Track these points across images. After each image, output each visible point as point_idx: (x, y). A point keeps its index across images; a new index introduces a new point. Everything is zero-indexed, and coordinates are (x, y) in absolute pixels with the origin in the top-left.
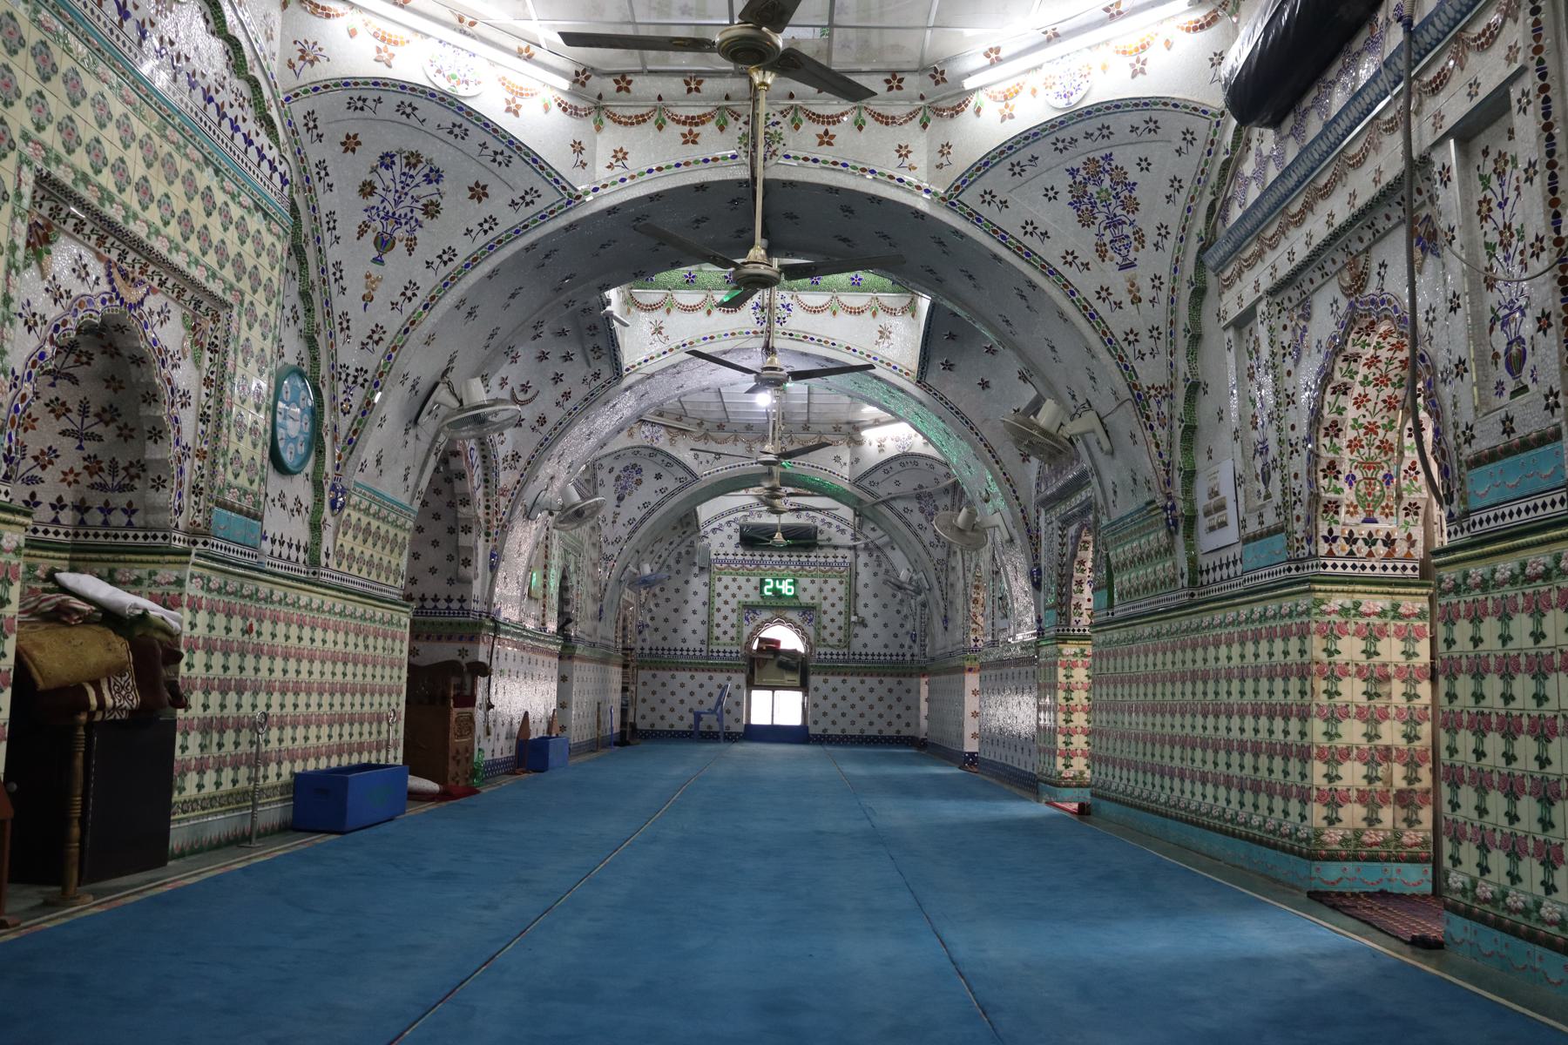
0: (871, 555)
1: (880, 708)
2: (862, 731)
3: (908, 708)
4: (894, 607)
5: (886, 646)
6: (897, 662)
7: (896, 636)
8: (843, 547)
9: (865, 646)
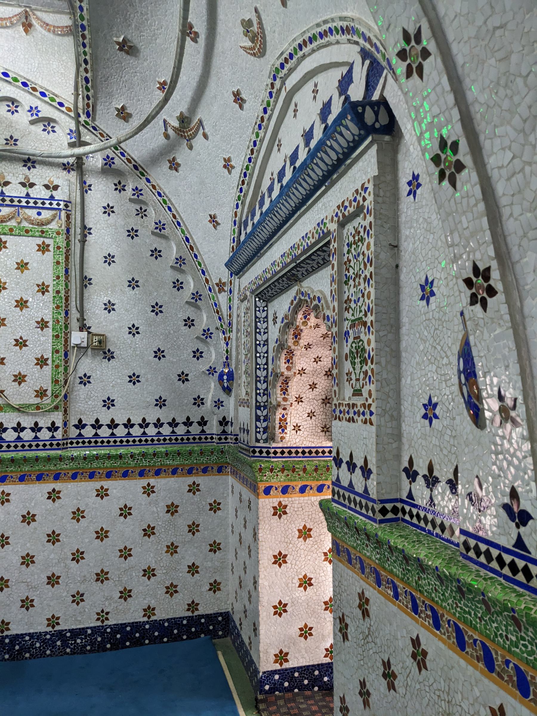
0: (120, 188)
1: (148, 553)
2: (102, 615)
3: (215, 547)
4: (177, 307)
5: (161, 403)
6: (187, 439)
7: (183, 378)
8: (47, 162)
9: (109, 403)
